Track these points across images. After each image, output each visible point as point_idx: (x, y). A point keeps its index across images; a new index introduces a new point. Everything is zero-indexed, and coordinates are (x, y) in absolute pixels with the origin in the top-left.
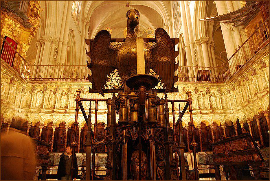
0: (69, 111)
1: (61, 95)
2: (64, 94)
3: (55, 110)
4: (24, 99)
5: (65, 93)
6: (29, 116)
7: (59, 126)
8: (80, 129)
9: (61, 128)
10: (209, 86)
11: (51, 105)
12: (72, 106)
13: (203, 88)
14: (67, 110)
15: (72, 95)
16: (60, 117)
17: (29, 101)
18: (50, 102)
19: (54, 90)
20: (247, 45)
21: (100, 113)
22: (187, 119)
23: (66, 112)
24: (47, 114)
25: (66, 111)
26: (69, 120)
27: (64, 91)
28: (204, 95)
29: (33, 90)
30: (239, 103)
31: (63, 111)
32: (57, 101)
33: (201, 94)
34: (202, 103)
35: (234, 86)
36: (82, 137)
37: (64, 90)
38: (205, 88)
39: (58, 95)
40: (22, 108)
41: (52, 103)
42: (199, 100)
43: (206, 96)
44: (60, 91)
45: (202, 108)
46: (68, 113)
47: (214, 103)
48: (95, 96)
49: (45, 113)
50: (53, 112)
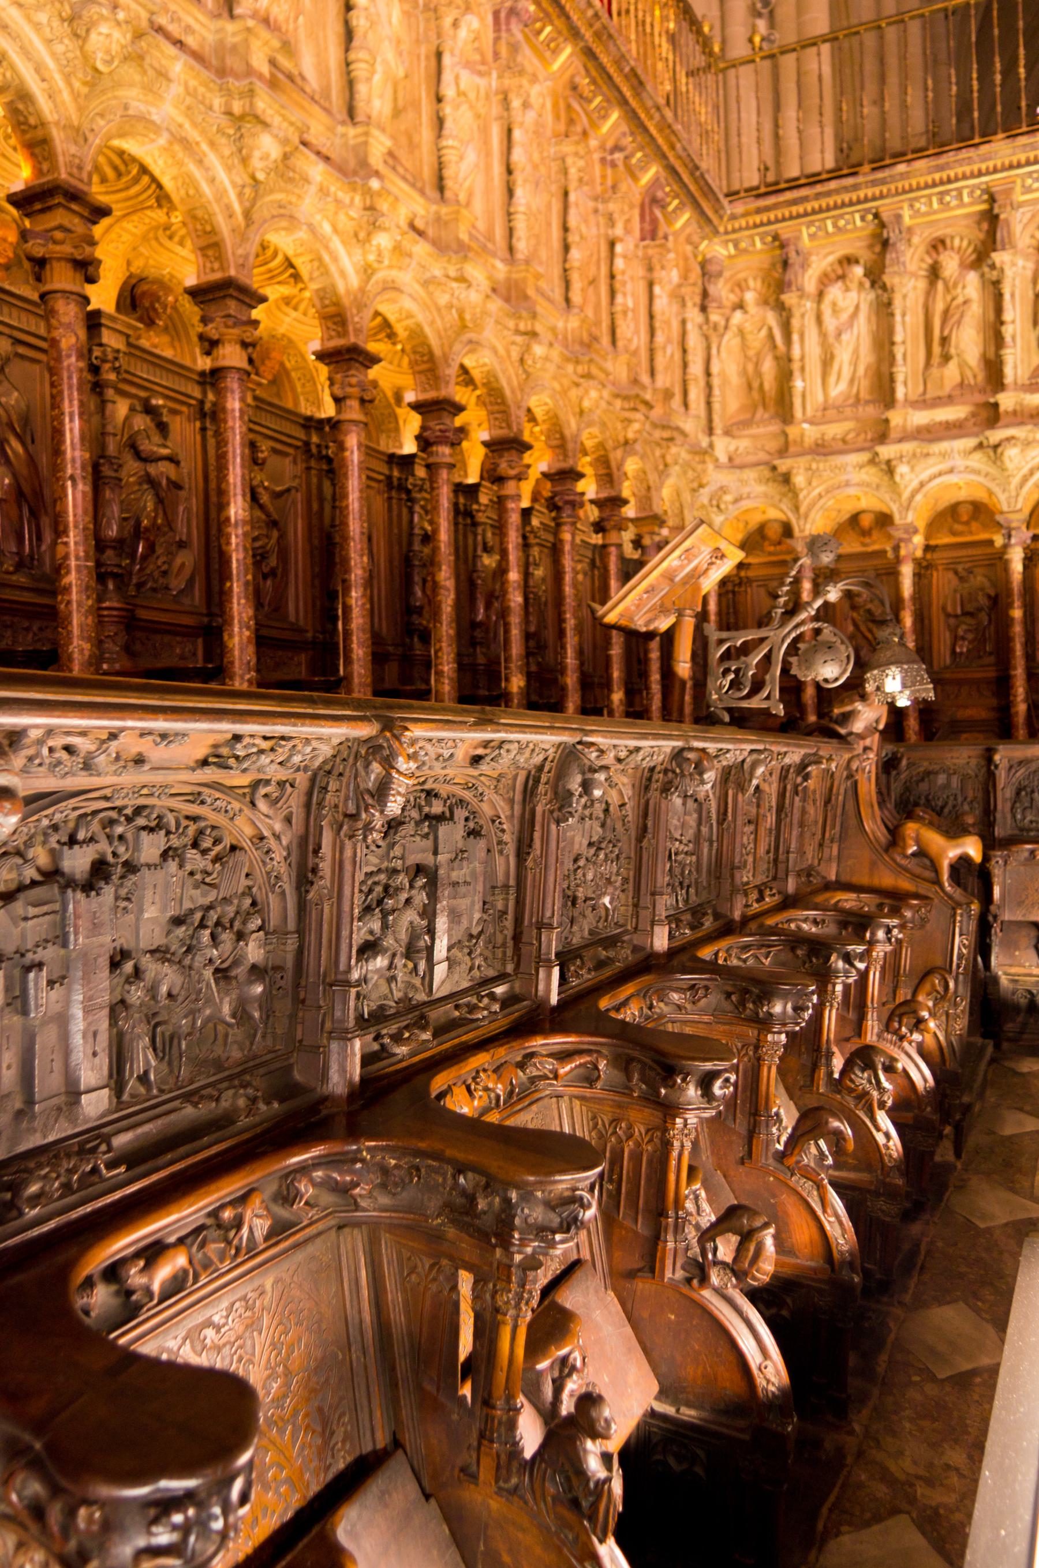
4: (728, 365)
6: (799, 480)
17: (768, 366)
18: (944, 341)
24: (944, 446)
29: (780, 274)
40: (727, 433)
41: (969, 343)
49: (929, 434)
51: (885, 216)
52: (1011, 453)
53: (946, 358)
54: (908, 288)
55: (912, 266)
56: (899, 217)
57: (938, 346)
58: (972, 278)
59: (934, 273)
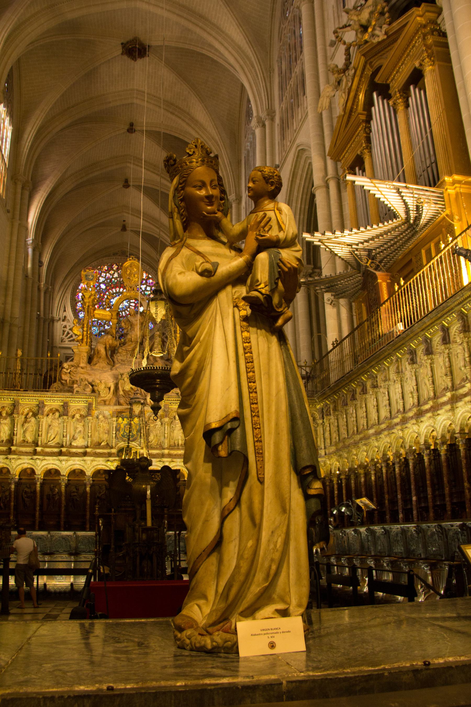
5: (7, 413)
8: (38, 483)
12: (22, 439)
14: (13, 448)
20: (346, 343)
21: (77, 454)
25: (10, 449)
30: (334, 440)
31: (4, 448)
35: (330, 407)
37: (4, 407)
46: (15, 453)
48: (67, 420)
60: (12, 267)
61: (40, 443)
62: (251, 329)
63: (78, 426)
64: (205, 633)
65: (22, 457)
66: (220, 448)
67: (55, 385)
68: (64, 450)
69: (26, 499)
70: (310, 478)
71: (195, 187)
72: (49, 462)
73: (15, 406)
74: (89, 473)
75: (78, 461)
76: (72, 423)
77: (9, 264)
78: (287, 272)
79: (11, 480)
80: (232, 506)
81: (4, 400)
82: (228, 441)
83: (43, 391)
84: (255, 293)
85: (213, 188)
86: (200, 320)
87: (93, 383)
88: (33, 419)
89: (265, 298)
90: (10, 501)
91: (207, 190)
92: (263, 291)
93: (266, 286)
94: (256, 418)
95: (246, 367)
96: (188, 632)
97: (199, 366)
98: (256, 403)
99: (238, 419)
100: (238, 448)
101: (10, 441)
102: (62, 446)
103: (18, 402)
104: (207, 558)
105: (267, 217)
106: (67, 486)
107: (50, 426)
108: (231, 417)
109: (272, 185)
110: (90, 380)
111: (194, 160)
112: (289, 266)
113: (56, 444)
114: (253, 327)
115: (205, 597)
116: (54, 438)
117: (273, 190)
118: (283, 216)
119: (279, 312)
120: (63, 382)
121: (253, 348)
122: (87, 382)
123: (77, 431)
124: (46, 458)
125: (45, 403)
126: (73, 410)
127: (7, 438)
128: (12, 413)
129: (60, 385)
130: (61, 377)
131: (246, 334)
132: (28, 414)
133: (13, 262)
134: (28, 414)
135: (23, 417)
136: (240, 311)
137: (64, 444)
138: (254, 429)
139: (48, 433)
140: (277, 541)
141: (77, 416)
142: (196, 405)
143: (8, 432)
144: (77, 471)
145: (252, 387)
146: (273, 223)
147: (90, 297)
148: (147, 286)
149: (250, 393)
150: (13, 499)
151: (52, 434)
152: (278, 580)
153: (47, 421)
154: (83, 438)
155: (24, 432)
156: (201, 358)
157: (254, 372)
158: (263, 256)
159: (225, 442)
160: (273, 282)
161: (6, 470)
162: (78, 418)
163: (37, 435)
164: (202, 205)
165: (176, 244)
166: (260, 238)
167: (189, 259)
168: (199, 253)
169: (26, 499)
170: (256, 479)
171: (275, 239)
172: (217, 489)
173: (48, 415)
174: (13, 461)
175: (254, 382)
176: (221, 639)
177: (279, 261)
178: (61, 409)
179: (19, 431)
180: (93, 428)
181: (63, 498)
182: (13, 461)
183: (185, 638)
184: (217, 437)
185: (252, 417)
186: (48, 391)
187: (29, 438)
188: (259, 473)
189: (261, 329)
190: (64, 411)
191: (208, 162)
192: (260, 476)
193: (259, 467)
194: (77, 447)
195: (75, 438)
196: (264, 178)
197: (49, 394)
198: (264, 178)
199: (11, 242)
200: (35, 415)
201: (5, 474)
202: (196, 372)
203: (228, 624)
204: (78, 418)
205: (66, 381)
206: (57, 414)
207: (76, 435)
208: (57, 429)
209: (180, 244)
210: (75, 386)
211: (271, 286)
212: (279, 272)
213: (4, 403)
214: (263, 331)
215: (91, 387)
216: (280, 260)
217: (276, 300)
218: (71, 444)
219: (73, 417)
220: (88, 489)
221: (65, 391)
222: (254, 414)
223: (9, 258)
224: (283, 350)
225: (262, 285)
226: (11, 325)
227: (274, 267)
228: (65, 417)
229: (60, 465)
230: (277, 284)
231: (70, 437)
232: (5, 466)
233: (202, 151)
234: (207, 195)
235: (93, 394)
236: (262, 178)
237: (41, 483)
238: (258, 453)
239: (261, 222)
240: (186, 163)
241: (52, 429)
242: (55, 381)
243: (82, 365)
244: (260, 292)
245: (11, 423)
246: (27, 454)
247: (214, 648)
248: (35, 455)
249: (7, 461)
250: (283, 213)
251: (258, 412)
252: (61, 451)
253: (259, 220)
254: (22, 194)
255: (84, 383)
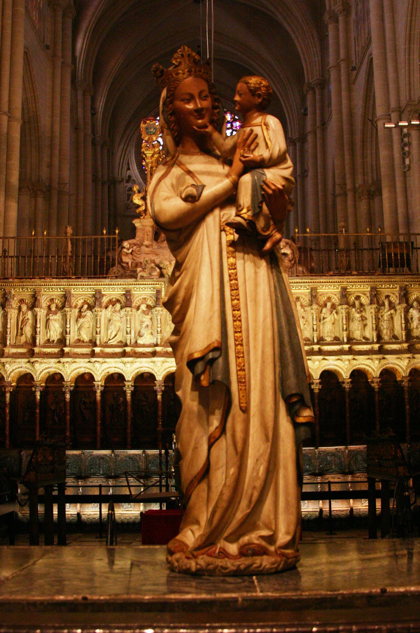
0: (70, 351)
1: (46, 312)
2: (53, 308)
3: (37, 350)
5: (57, 307)
7: (46, 383)
8: (99, 391)
9: (50, 389)
10: (407, 283)
11: (26, 337)
12: (76, 338)
13: (392, 288)
14: (66, 350)
15: (73, 310)
16: (50, 366)
18: (22, 329)
19: (28, 300)
21: (144, 354)
22: (346, 367)
23: (62, 354)
24: (19, 360)
25: (62, 351)
26: (71, 373)
27: (52, 300)
28: (392, 306)
31: (56, 350)
32: (41, 326)
33: (387, 303)
34: (385, 327)
36: (103, 410)
37: (53, 299)
38: (396, 288)
39: (41, 313)
41: (28, 330)
42: (379, 319)
43: (398, 307)
44: (44, 301)
45: (386, 337)
46: (68, 355)
47: (415, 326)
48: (130, 313)
50: (32, 354)
51: (7, 291)
52: (37, 365)
53: (22, 334)
54: (13, 314)
55: (14, 306)
56: (10, 292)
57: (20, 331)
58: (30, 313)
59: (20, 309)
60: (58, 119)
61: (98, 342)
62: (238, 254)
63: (144, 319)
64: (191, 556)
65: (77, 360)
66: (202, 378)
67: (115, 269)
68: (128, 349)
69: (85, 411)
70: (297, 407)
71: (182, 100)
72: (111, 365)
73: (66, 298)
74: (160, 377)
75: (146, 362)
76: (137, 316)
77: (52, 116)
78: (271, 195)
79: (66, 388)
80: (217, 435)
81: (53, 291)
82: (210, 371)
83: (99, 278)
84: (239, 219)
85: (202, 98)
86: (189, 245)
87: (161, 266)
88: (89, 313)
89: (248, 223)
90: (65, 414)
91: (196, 104)
92: (245, 216)
93: (248, 211)
94: (239, 347)
95: (231, 295)
96: (177, 556)
97: (186, 293)
98: (240, 332)
99: (221, 348)
100: (219, 377)
101: (62, 342)
102: (126, 345)
103: (70, 292)
104: (198, 484)
105: (254, 133)
106: (133, 393)
107: (110, 320)
108: (212, 347)
109: (259, 98)
110: (157, 261)
111: (181, 71)
112: (273, 187)
113: (118, 342)
114: (239, 252)
115: (198, 522)
116: (116, 335)
117: (261, 103)
118: (271, 132)
119: (265, 236)
120: (124, 265)
121: (238, 274)
122: (153, 265)
123: (144, 326)
124: (107, 360)
125: (103, 293)
126: (137, 299)
127: (59, 337)
128: (63, 307)
129: (120, 269)
130: (121, 259)
131: (232, 260)
132: (82, 307)
133: (57, 112)
134: (82, 307)
135: (77, 310)
136: (227, 235)
137: (128, 343)
138: (237, 357)
139: (108, 329)
140: (259, 469)
141: (143, 307)
142: (184, 333)
143: (59, 330)
144: (145, 375)
145: (237, 315)
146: (260, 140)
147: (153, 156)
148: (233, 130)
149: (234, 321)
150: (68, 412)
151: (112, 331)
152: (262, 508)
153: (106, 315)
154: (152, 334)
155: (79, 329)
156: (188, 285)
157: (238, 300)
158: (247, 178)
159: (207, 372)
160: (256, 206)
161: (59, 376)
162: (145, 309)
163: (95, 332)
164: (192, 118)
165: (167, 162)
166: (243, 159)
167: (180, 180)
168: (189, 173)
169: (85, 411)
170: (238, 408)
171: (259, 158)
172: (205, 416)
173: (106, 307)
174: (66, 365)
175: (238, 310)
176: (205, 561)
177: (262, 184)
178: (123, 299)
179: (73, 328)
180: (163, 322)
181: (129, 409)
182: (66, 365)
183: (174, 561)
184: (200, 367)
185: (236, 345)
186: (105, 278)
187: (86, 337)
188: (241, 401)
189: (248, 254)
190: (127, 301)
191: (195, 72)
192: (242, 405)
193: (241, 396)
194: (144, 346)
195: (141, 334)
196: (251, 91)
197: (107, 281)
198: (251, 91)
199: (53, 88)
200: (90, 308)
201: (58, 381)
202: (184, 300)
203: (214, 549)
204: (145, 309)
205: (128, 263)
206: (118, 306)
207: (143, 331)
208: (118, 324)
209: (172, 162)
210: (139, 269)
211: (254, 211)
212: (263, 195)
213: (53, 295)
214: (251, 256)
215: (158, 270)
216: (264, 182)
217: (261, 224)
218: (136, 342)
219: (138, 308)
220: (159, 397)
221: (126, 277)
222: (238, 343)
223: (53, 107)
224: (274, 274)
225: (245, 211)
226: (60, 192)
227: (257, 190)
228: (128, 309)
229: (124, 369)
230: (261, 208)
231: (135, 333)
232: (58, 371)
233: (189, 61)
234: (195, 108)
235: (161, 279)
236: (247, 90)
237: (101, 392)
238: (241, 382)
239: (247, 139)
240: (172, 75)
241: (113, 325)
242: (113, 265)
243: (146, 243)
244: (243, 218)
245: (63, 319)
246: (83, 356)
247: (198, 570)
248: (93, 357)
249: (60, 366)
250: (270, 128)
251: (242, 340)
252: (125, 350)
253: (245, 137)
254: (63, 23)
255: (150, 266)
